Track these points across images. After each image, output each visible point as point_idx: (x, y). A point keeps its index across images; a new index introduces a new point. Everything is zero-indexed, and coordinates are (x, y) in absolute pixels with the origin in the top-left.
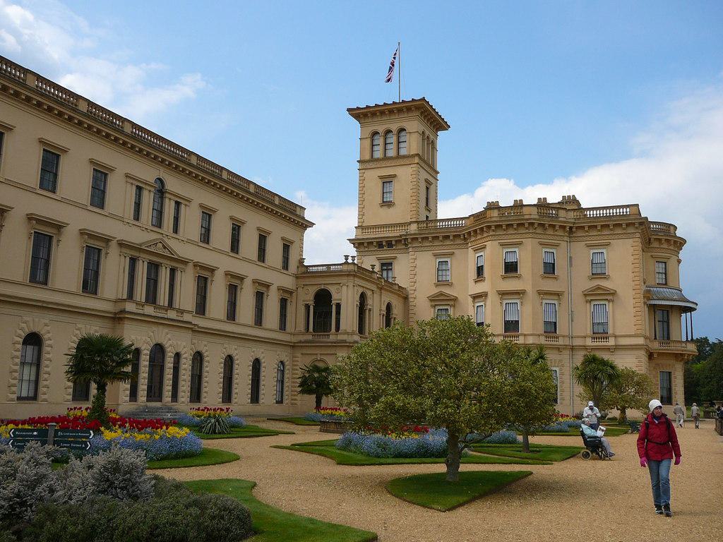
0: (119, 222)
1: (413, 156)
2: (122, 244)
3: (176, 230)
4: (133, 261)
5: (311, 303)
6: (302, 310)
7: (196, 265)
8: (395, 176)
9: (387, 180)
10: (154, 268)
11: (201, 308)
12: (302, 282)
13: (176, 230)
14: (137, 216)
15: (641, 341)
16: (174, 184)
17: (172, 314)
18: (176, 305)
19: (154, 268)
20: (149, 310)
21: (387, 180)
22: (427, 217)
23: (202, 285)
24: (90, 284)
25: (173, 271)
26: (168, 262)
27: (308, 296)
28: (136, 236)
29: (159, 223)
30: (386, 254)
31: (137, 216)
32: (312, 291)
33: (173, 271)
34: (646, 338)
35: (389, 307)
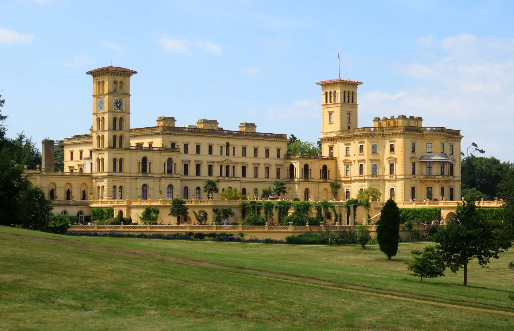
0: (217, 157)
1: (339, 103)
2: (218, 162)
3: (234, 155)
4: (221, 166)
5: (289, 168)
6: (286, 171)
7: (241, 163)
8: (333, 112)
9: (331, 113)
10: (227, 167)
11: (244, 175)
12: (286, 161)
13: (234, 155)
14: (221, 154)
15: (403, 177)
16: (232, 142)
17: (234, 179)
18: (235, 176)
19: (227, 167)
20: (226, 178)
21: (331, 113)
22: (349, 127)
23: (244, 169)
24: (210, 173)
25: (234, 167)
27: (287, 166)
28: (221, 159)
29: (228, 154)
30: (331, 144)
31: (221, 154)
32: (289, 164)
33: (234, 167)
34: (404, 175)
35: (325, 167)
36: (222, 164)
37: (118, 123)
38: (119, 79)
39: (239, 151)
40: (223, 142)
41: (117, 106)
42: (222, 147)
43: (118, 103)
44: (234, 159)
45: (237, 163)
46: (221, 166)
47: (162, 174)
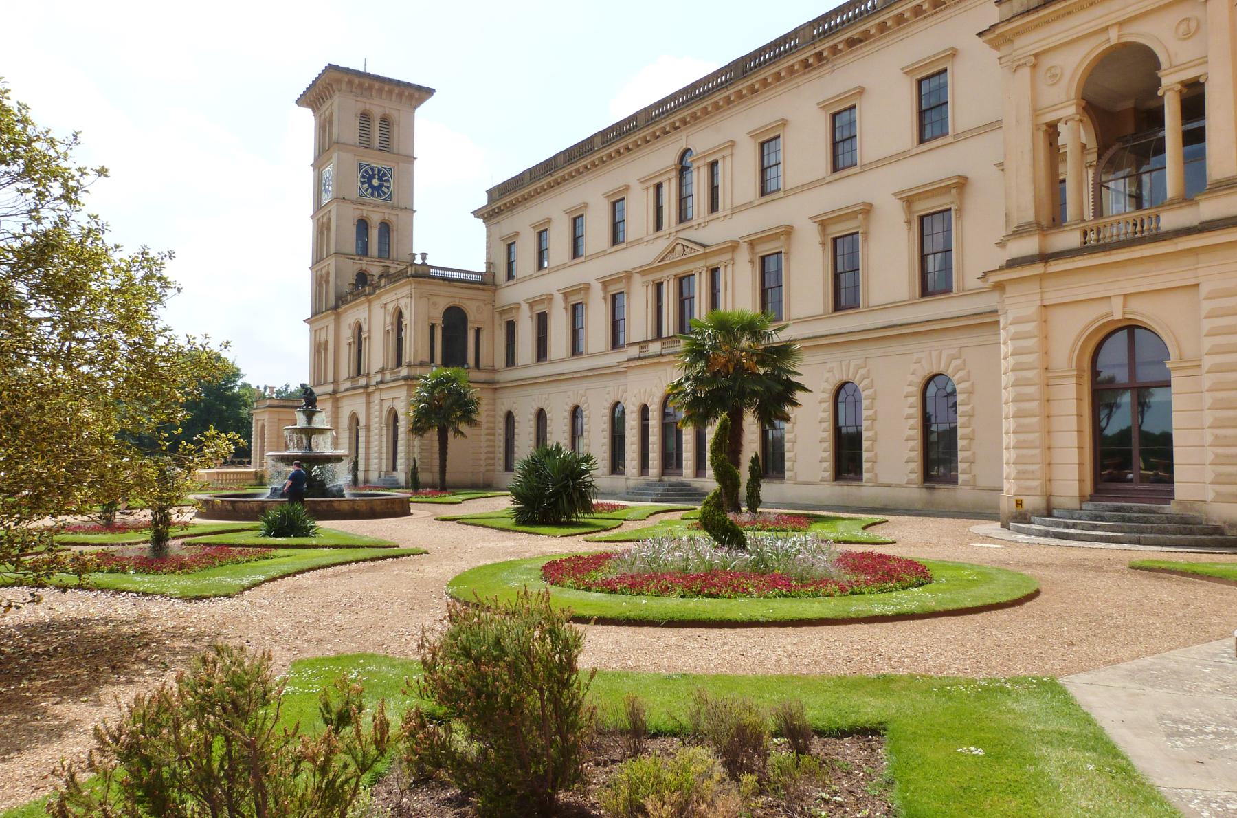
2: (644, 272)
14: (659, 226)
16: (702, 140)
26: (702, 264)
31: (659, 226)
36: (656, 276)
37: (374, 234)
38: (377, 107)
39: (740, 178)
40: (662, 157)
41: (371, 186)
42: (659, 187)
43: (372, 177)
44: (714, 232)
45: (734, 247)
46: (659, 286)
47: (422, 364)
